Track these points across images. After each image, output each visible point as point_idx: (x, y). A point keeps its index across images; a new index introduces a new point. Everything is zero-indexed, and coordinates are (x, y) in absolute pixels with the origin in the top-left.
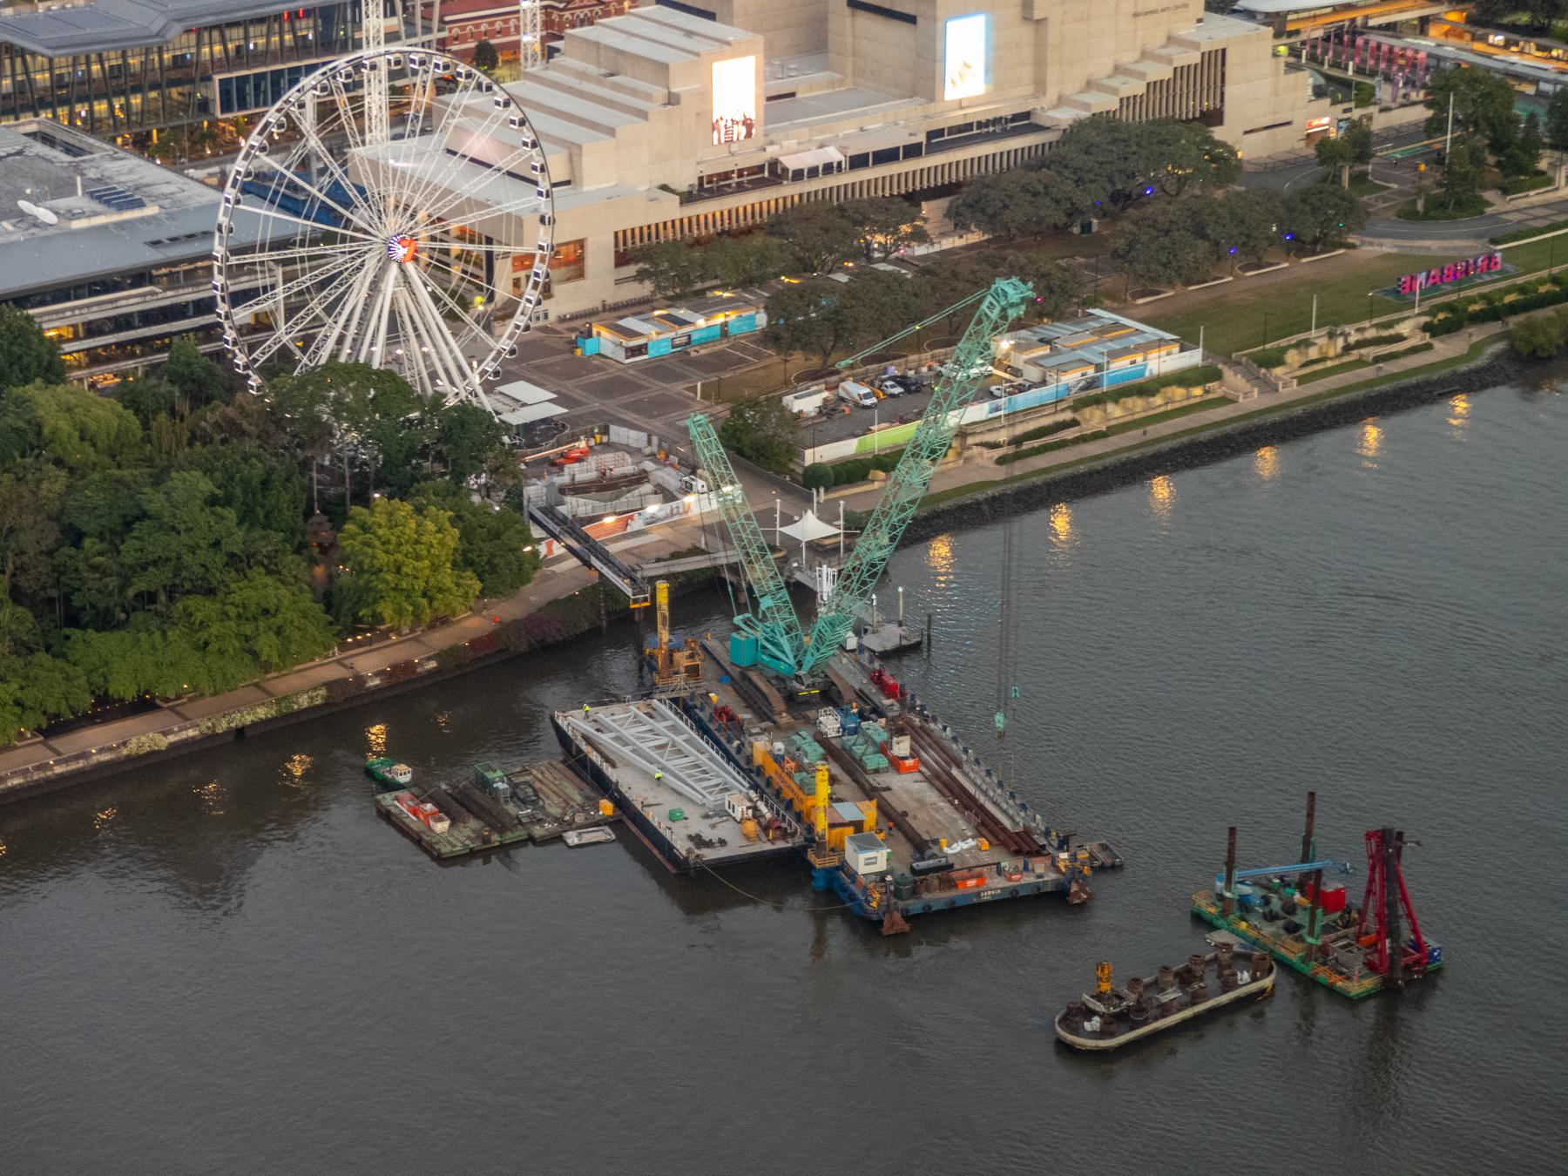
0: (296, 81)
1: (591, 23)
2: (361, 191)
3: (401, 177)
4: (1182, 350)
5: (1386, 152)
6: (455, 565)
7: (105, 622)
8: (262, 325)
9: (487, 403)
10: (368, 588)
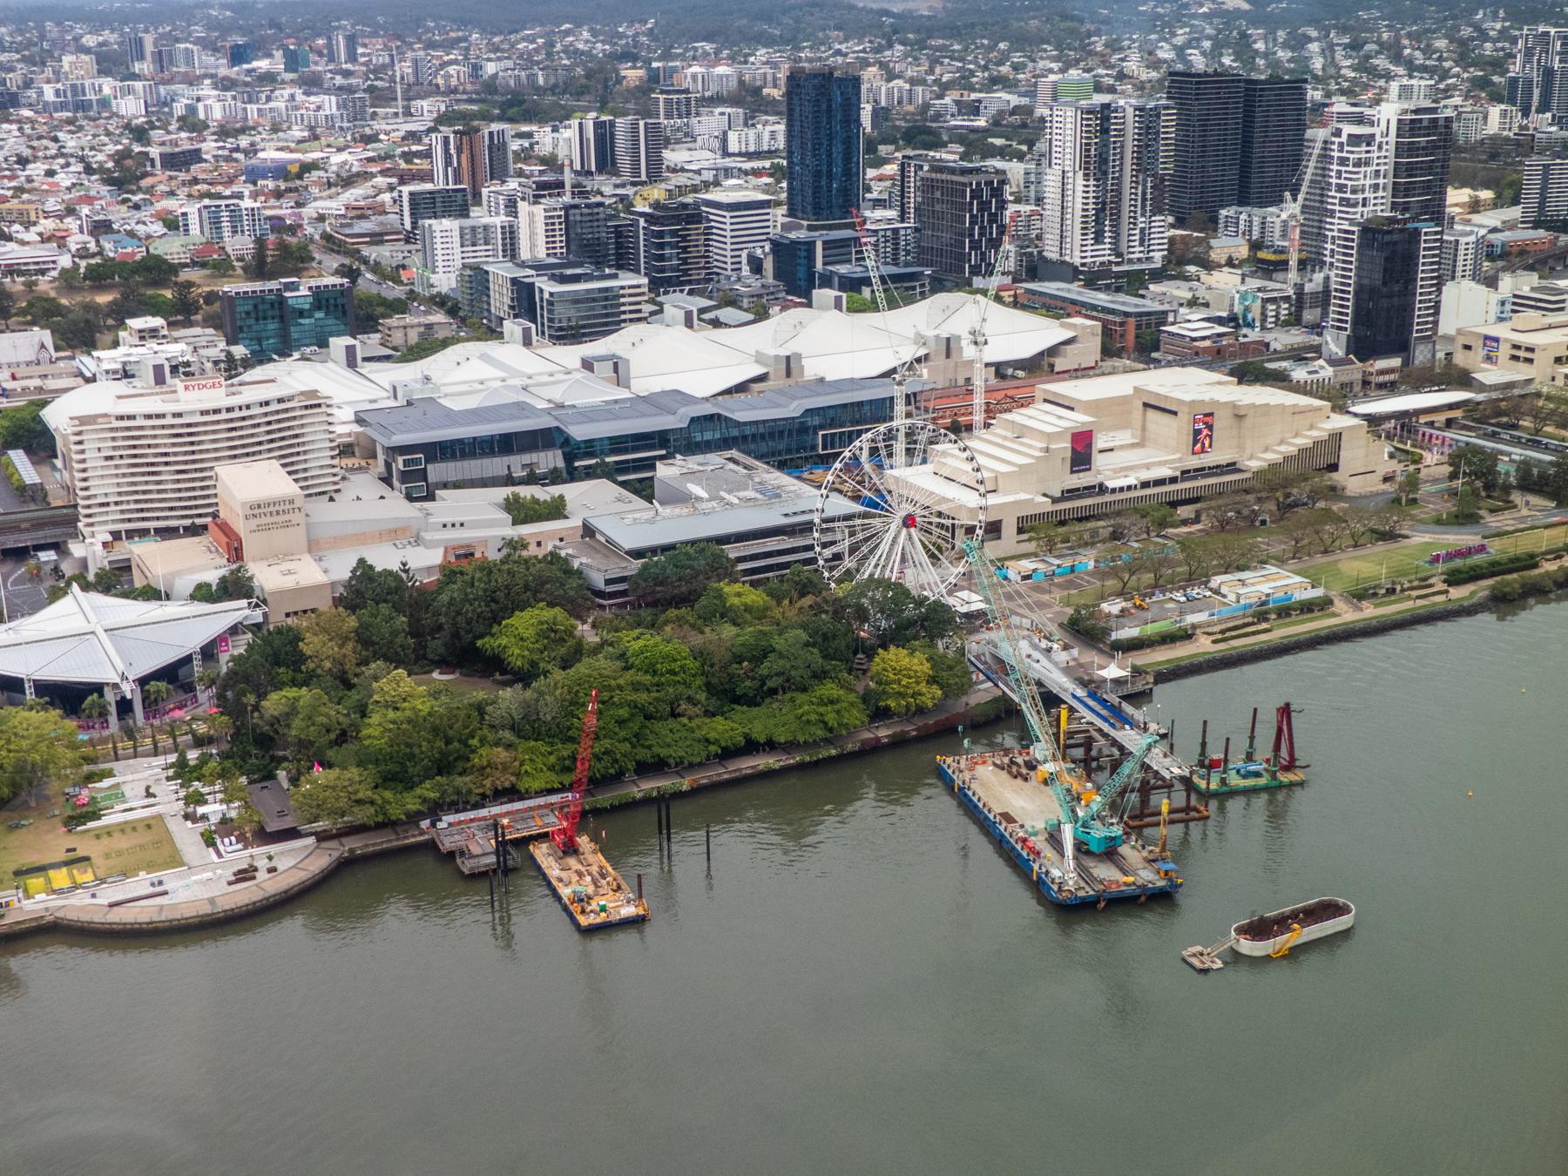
0: (860, 436)
1: (1009, 410)
2: (890, 492)
3: (911, 486)
4: (1313, 587)
5: (1426, 489)
6: (928, 682)
7: (752, 702)
8: (838, 557)
9: (950, 601)
10: (884, 692)
